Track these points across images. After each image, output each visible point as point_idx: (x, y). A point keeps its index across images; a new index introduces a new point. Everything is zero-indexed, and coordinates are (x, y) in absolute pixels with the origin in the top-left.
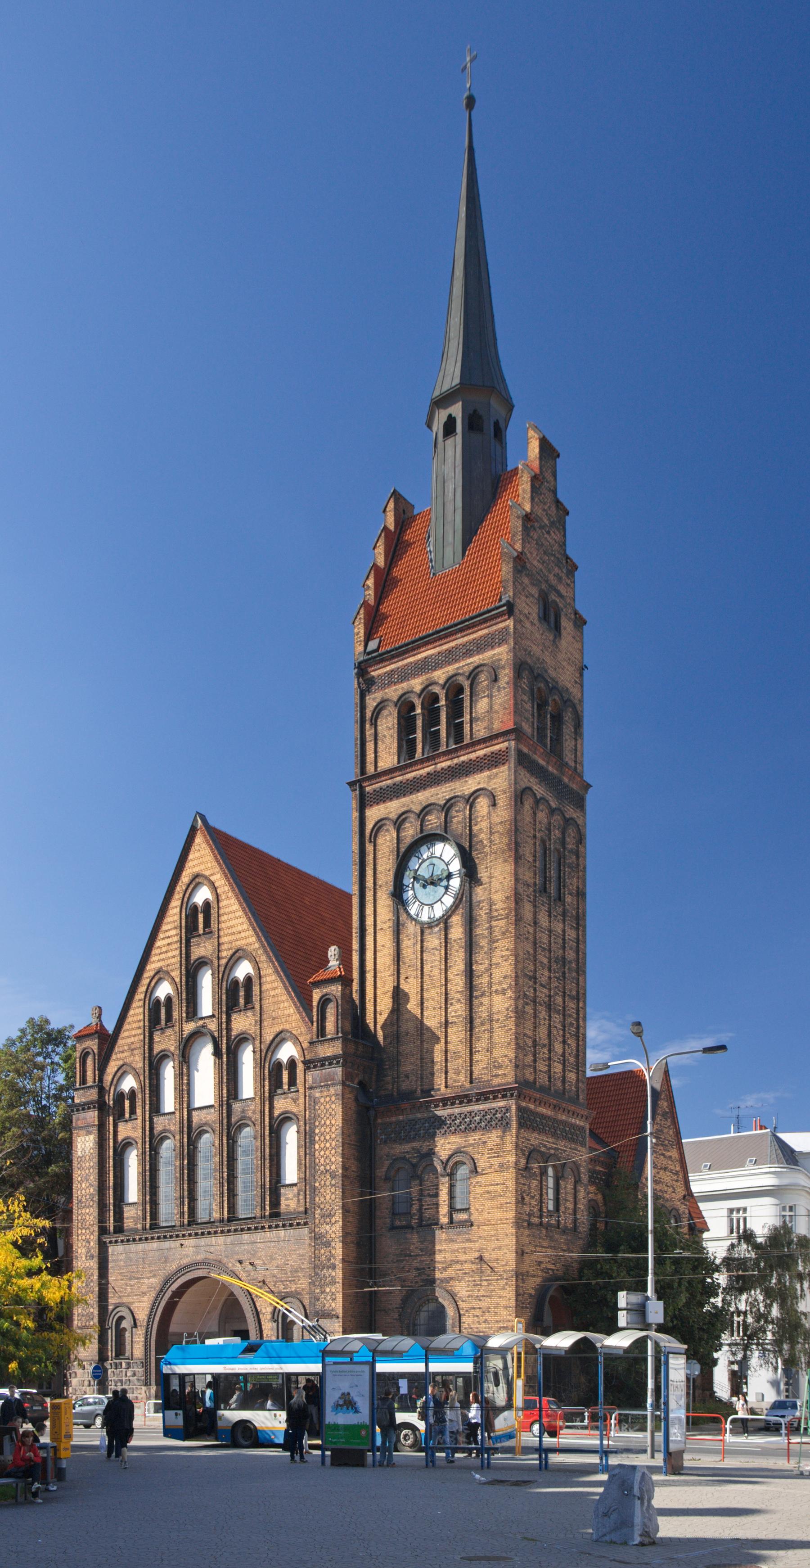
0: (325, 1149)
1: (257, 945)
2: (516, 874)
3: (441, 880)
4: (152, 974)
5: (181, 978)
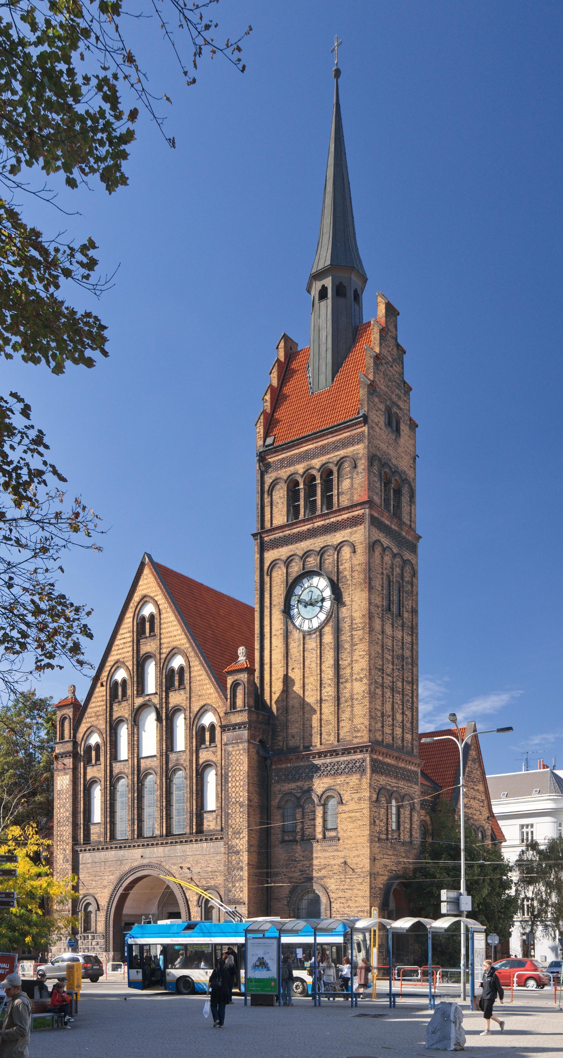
0: (236, 787)
1: (187, 645)
2: (370, 599)
3: (317, 602)
4: (112, 663)
5: (133, 667)
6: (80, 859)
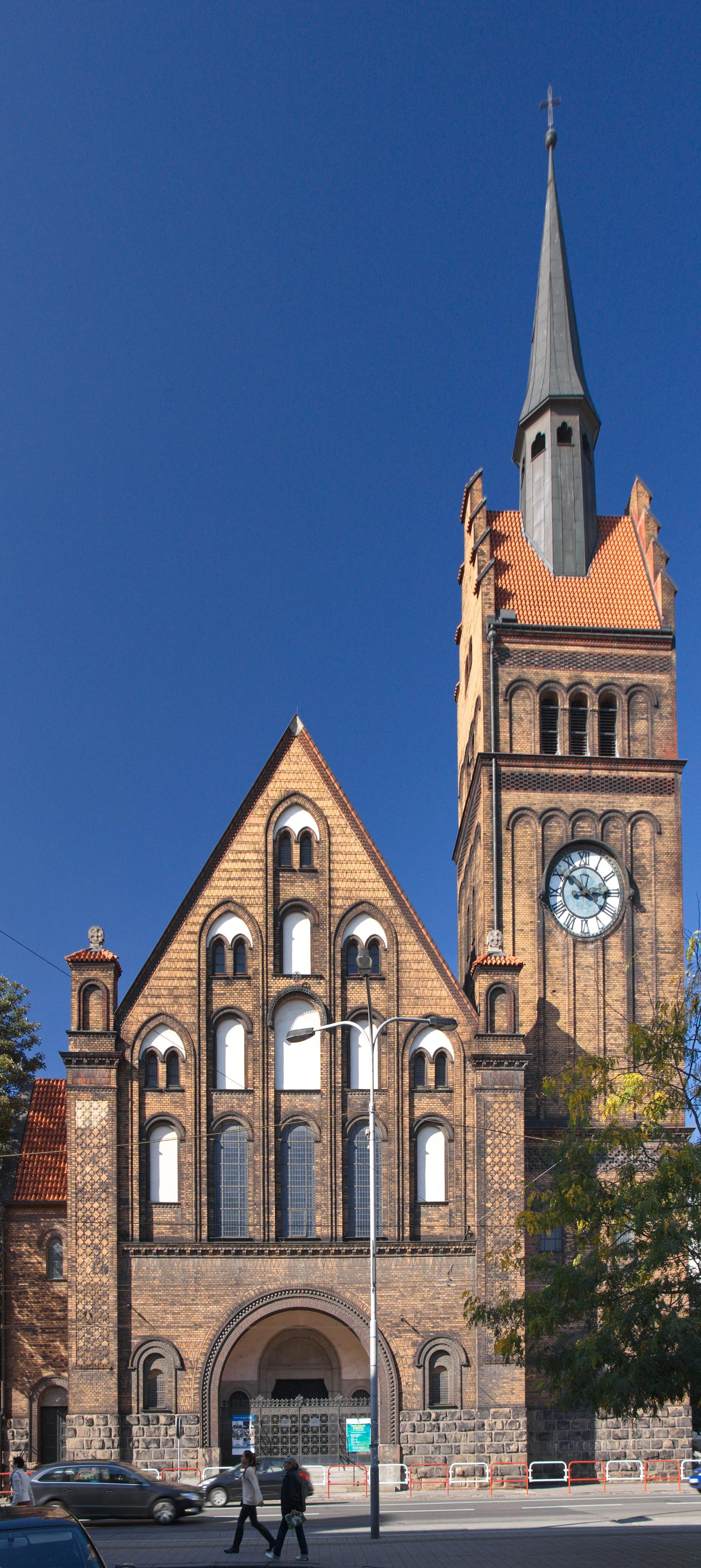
6: (133, 1269)
